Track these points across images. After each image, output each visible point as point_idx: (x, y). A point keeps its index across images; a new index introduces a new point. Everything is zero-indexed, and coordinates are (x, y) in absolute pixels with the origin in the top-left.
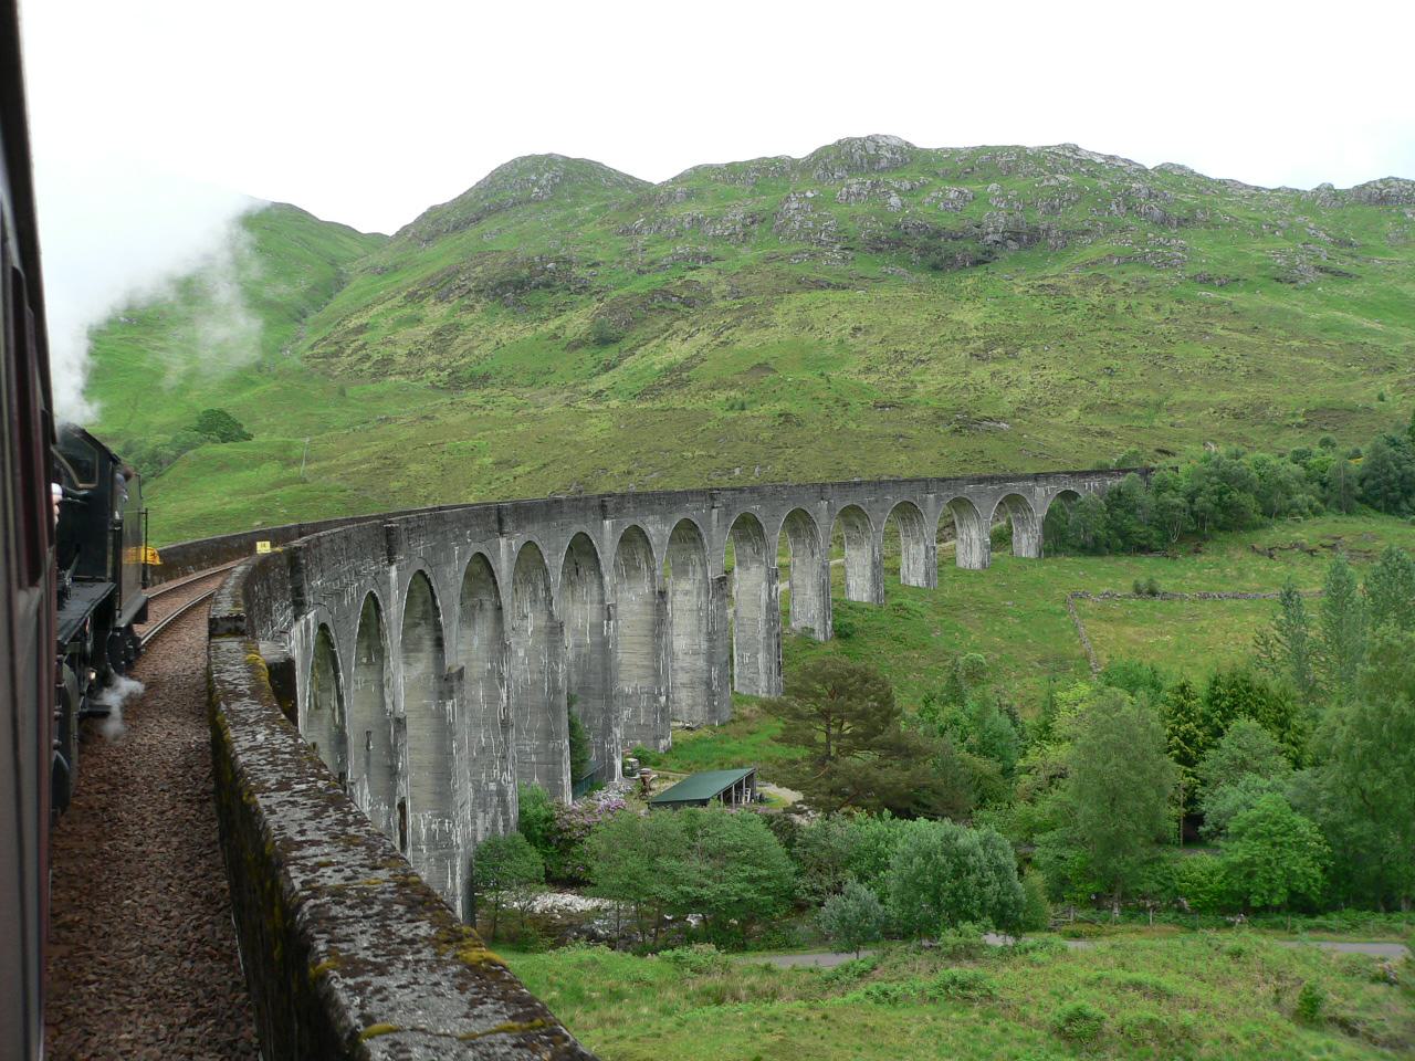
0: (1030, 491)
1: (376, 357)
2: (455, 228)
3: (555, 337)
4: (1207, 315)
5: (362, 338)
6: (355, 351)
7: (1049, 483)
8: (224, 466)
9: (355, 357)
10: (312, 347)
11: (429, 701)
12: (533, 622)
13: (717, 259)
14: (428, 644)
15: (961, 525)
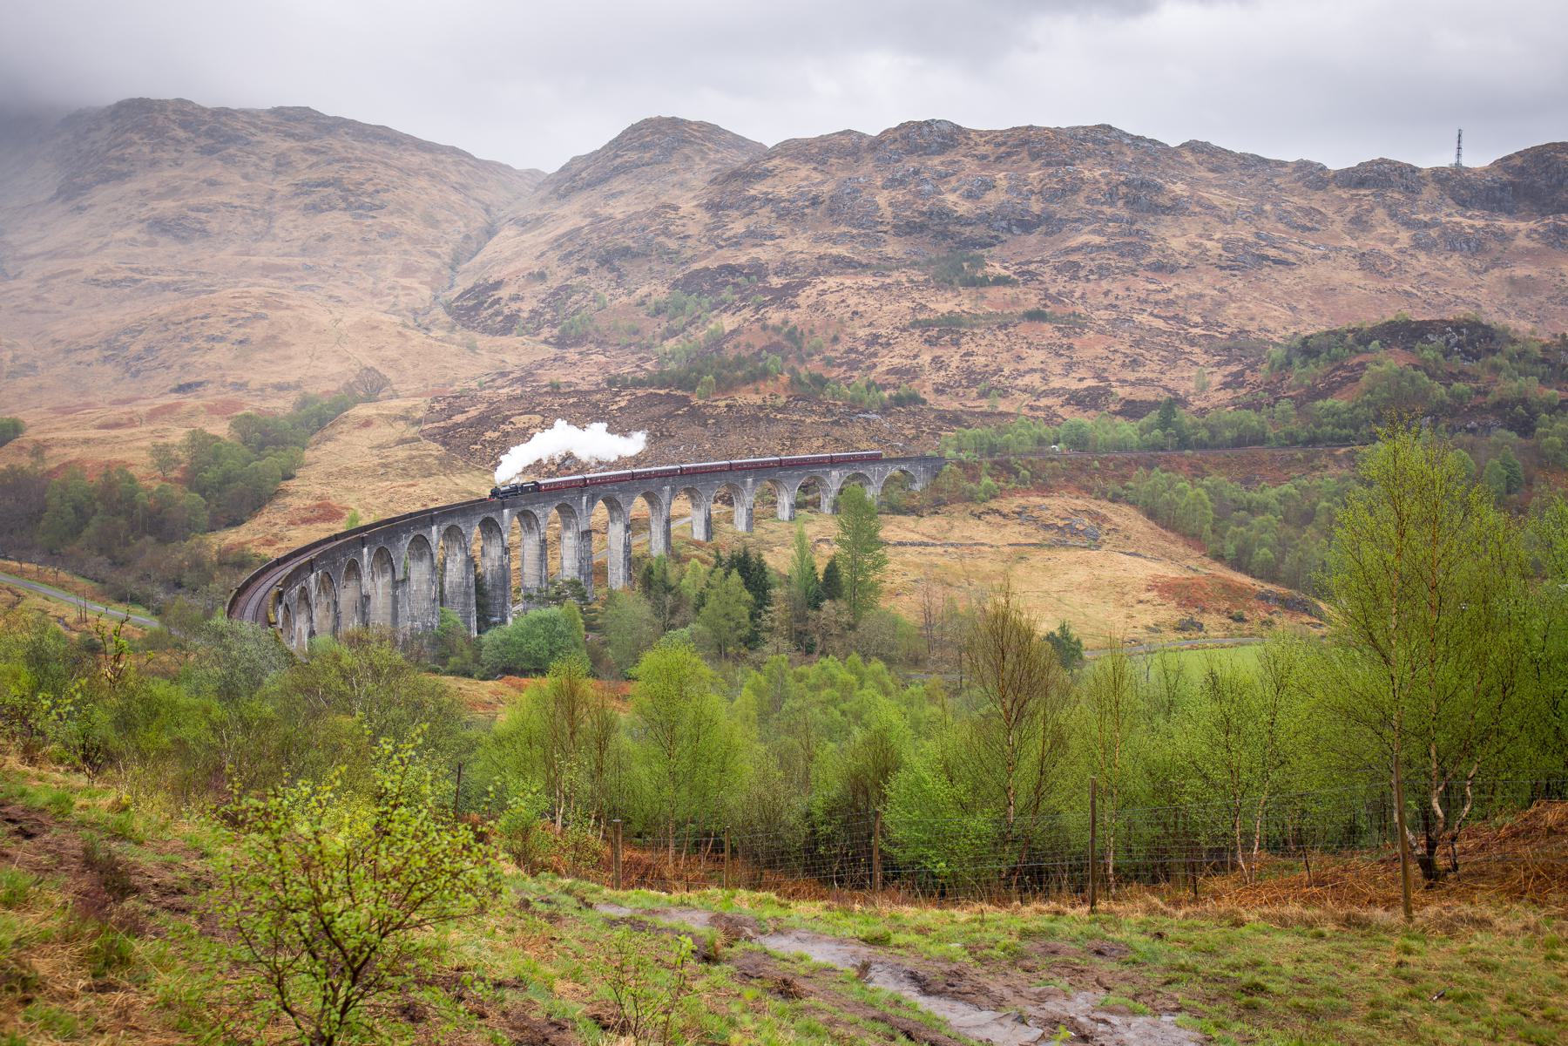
1: (506, 311)
2: (589, 185)
3: (643, 303)
4: (1146, 301)
8: (367, 423)
9: (490, 311)
11: (390, 591)
12: (460, 557)
13: (780, 237)
14: (390, 570)
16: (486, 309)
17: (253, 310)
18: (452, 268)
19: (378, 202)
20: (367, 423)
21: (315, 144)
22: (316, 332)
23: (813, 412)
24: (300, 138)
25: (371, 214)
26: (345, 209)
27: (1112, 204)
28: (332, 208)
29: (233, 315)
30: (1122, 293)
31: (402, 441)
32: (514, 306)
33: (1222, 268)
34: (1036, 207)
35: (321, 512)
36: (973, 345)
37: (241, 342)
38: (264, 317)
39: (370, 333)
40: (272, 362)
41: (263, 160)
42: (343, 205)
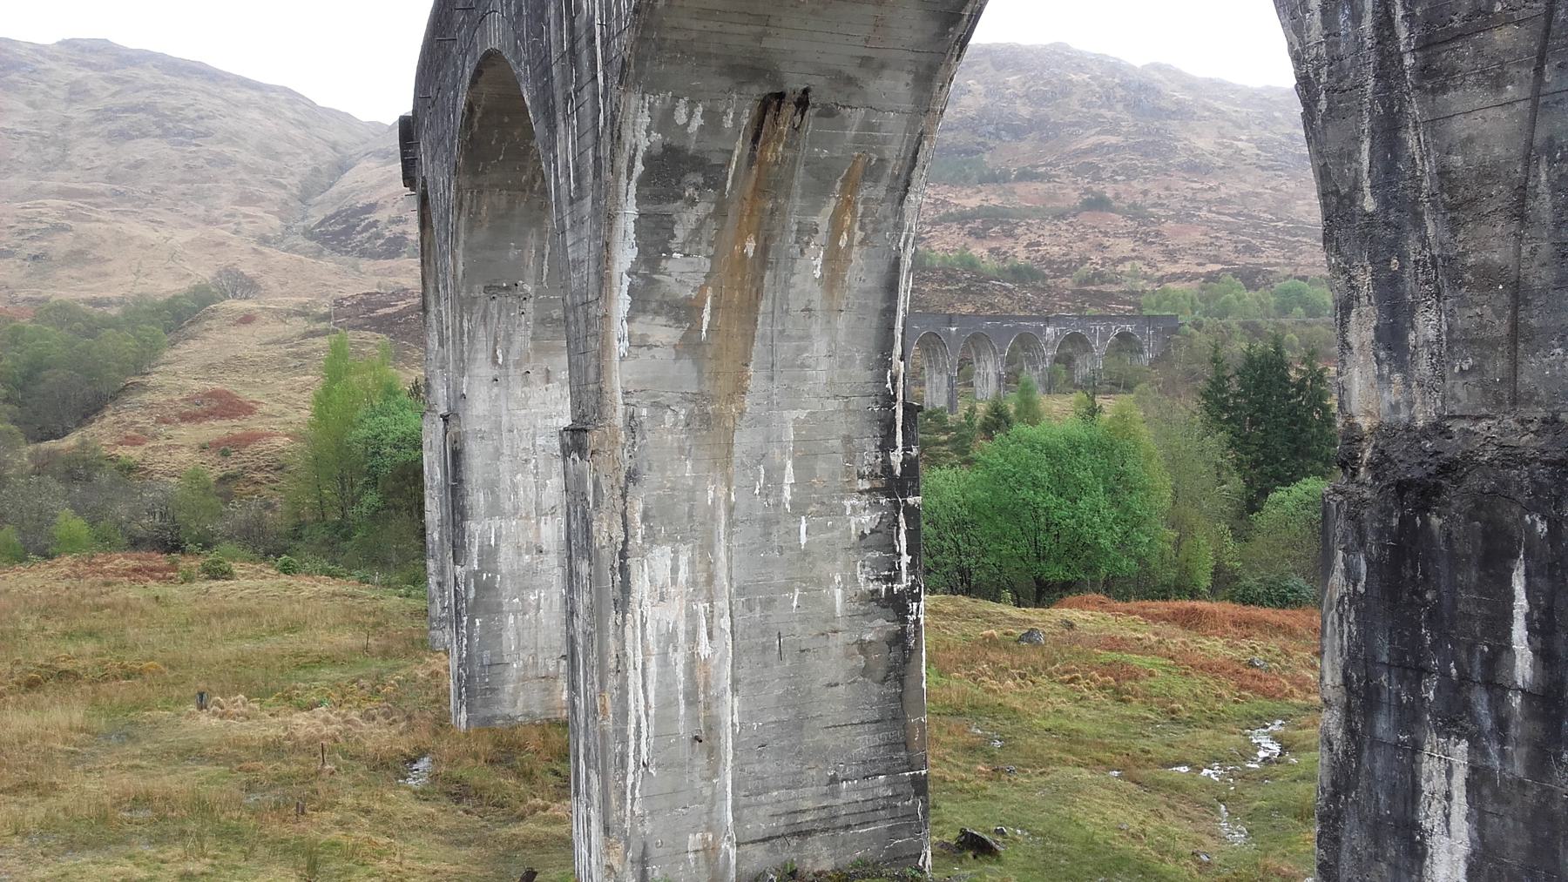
0: (1041, 331)
5: (372, 217)
6: (365, 229)
7: (1059, 325)
8: (247, 319)
10: (322, 223)
15: (978, 360)
16: (359, 233)
17: (50, 220)
18: (302, 201)
19: (202, 130)
20: (247, 319)
21: (117, 73)
22: (141, 247)
23: (929, 279)
24: (101, 68)
25: (194, 141)
26: (160, 136)
27: (1111, 108)
28: (145, 135)
29: (23, 226)
30: (1163, 193)
31: (314, 334)
32: (397, 229)
33: (1263, 168)
34: (1025, 111)
35: (215, 404)
36: (1033, 236)
37: (35, 257)
38: (69, 229)
39: (214, 250)
40: (80, 280)
41: (53, 87)
42: (159, 132)
